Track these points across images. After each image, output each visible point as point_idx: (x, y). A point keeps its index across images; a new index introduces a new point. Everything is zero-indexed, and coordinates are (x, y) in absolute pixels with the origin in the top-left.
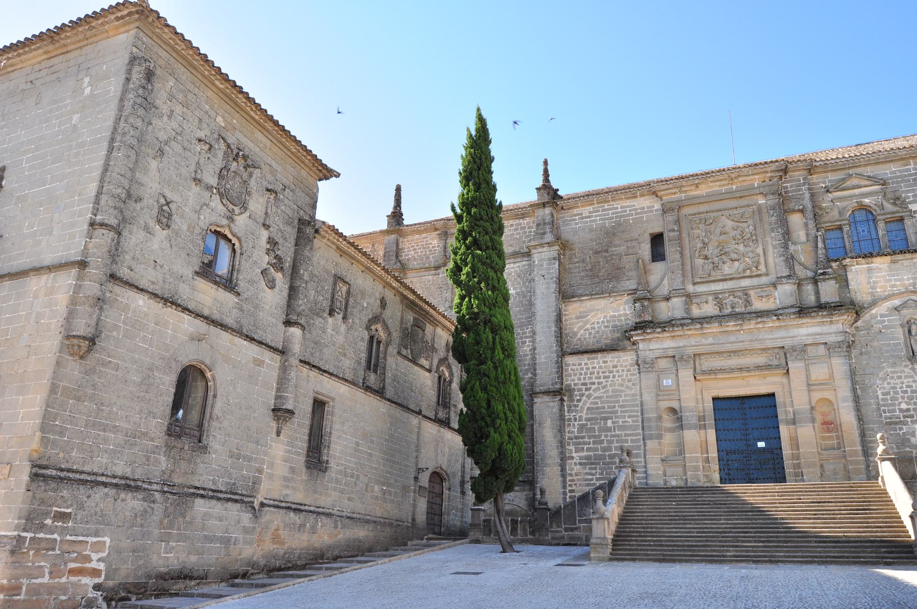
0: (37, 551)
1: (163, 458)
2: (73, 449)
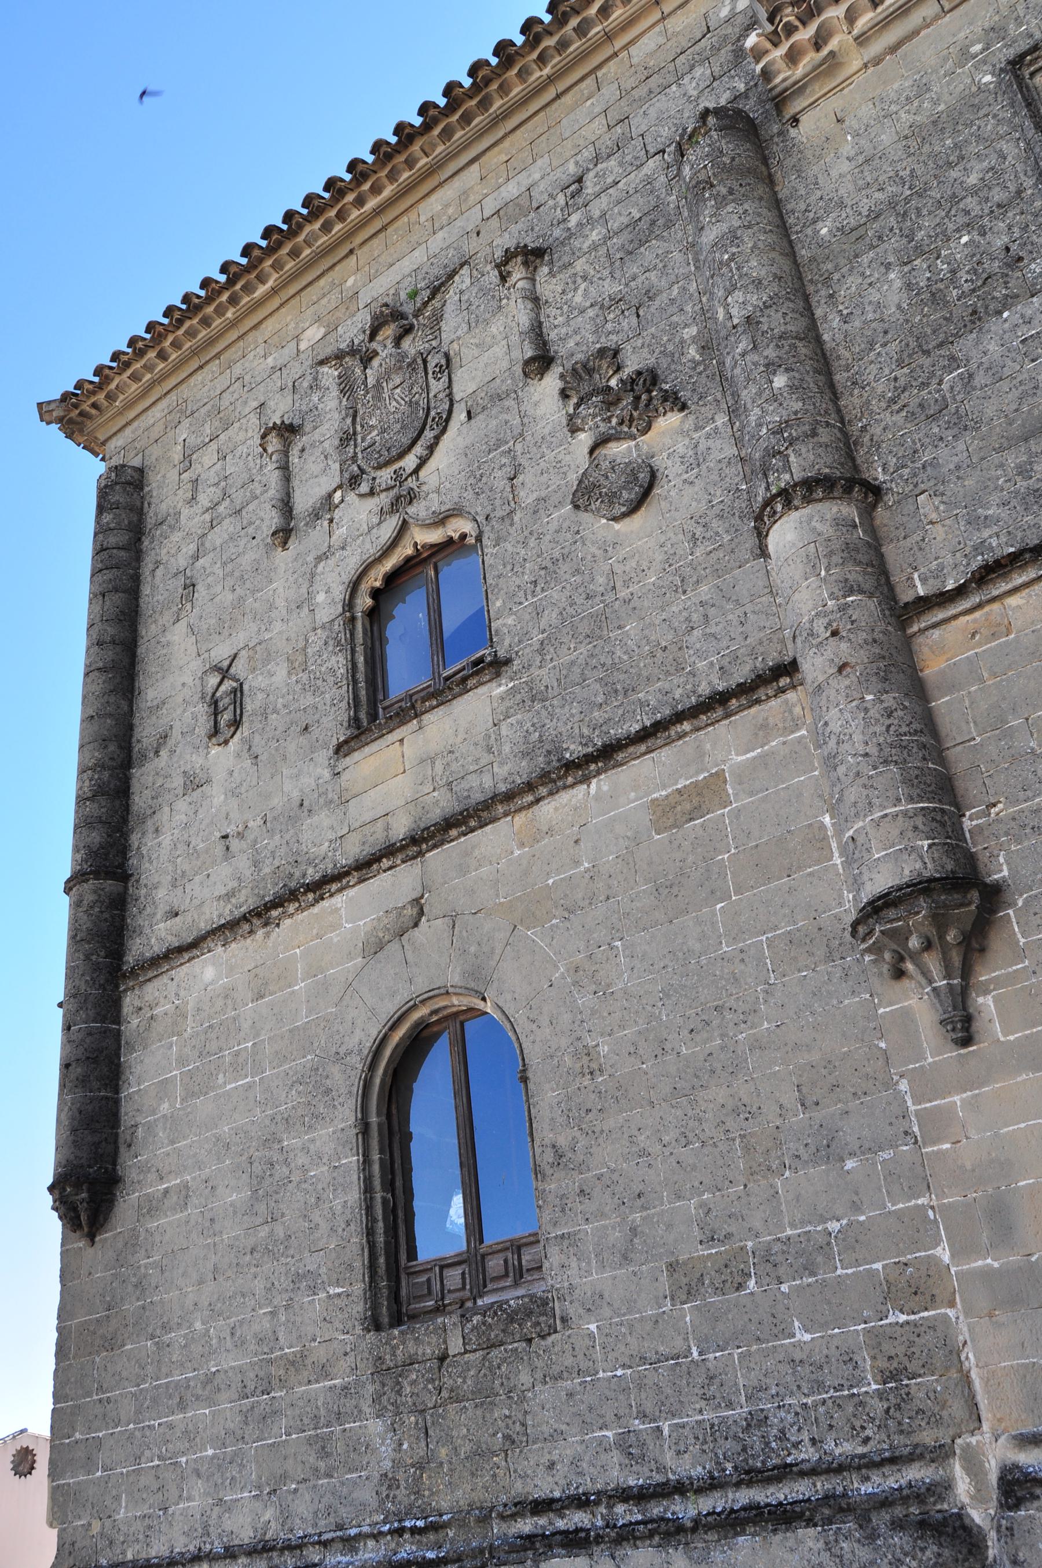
2: (117, 1498)
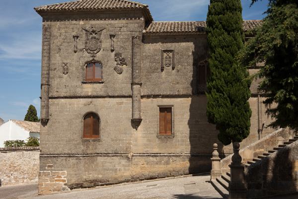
1: (82, 146)
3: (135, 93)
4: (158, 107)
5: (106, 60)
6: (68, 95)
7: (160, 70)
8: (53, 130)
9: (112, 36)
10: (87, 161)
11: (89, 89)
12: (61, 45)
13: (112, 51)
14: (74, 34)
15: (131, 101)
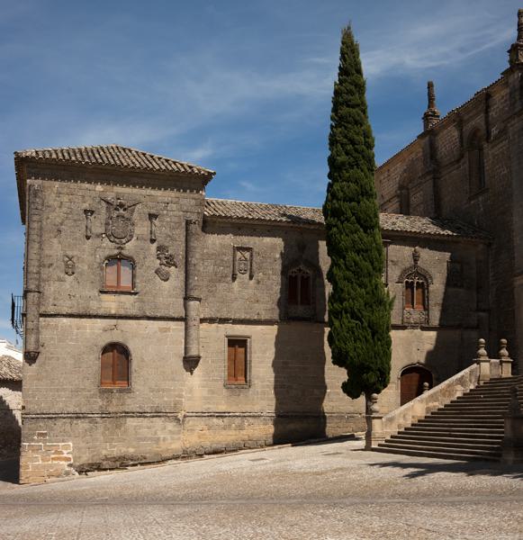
0: (33, 451)
1: (99, 400)
3: (193, 314)
4: (226, 339)
5: (141, 257)
6: (74, 311)
7: (230, 279)
8: (46, 371)
9: (152, 217)
10: (109, 426)
11: (111, 303)
12: (61, 224)
13: (153, 241)
14: (86, 206)
15: (184, 327)
